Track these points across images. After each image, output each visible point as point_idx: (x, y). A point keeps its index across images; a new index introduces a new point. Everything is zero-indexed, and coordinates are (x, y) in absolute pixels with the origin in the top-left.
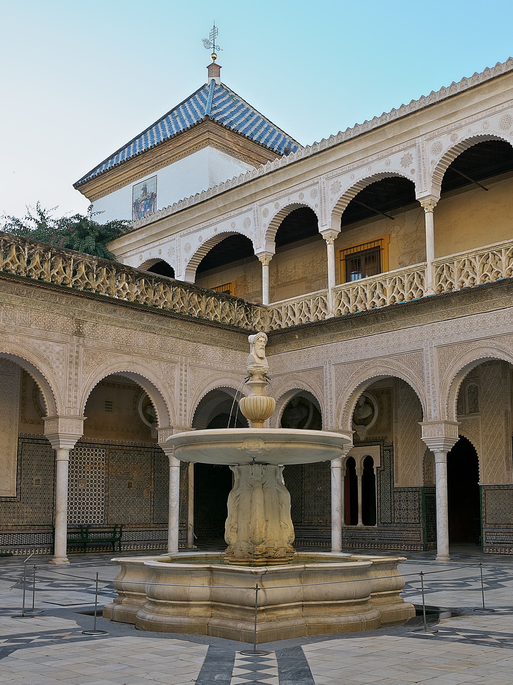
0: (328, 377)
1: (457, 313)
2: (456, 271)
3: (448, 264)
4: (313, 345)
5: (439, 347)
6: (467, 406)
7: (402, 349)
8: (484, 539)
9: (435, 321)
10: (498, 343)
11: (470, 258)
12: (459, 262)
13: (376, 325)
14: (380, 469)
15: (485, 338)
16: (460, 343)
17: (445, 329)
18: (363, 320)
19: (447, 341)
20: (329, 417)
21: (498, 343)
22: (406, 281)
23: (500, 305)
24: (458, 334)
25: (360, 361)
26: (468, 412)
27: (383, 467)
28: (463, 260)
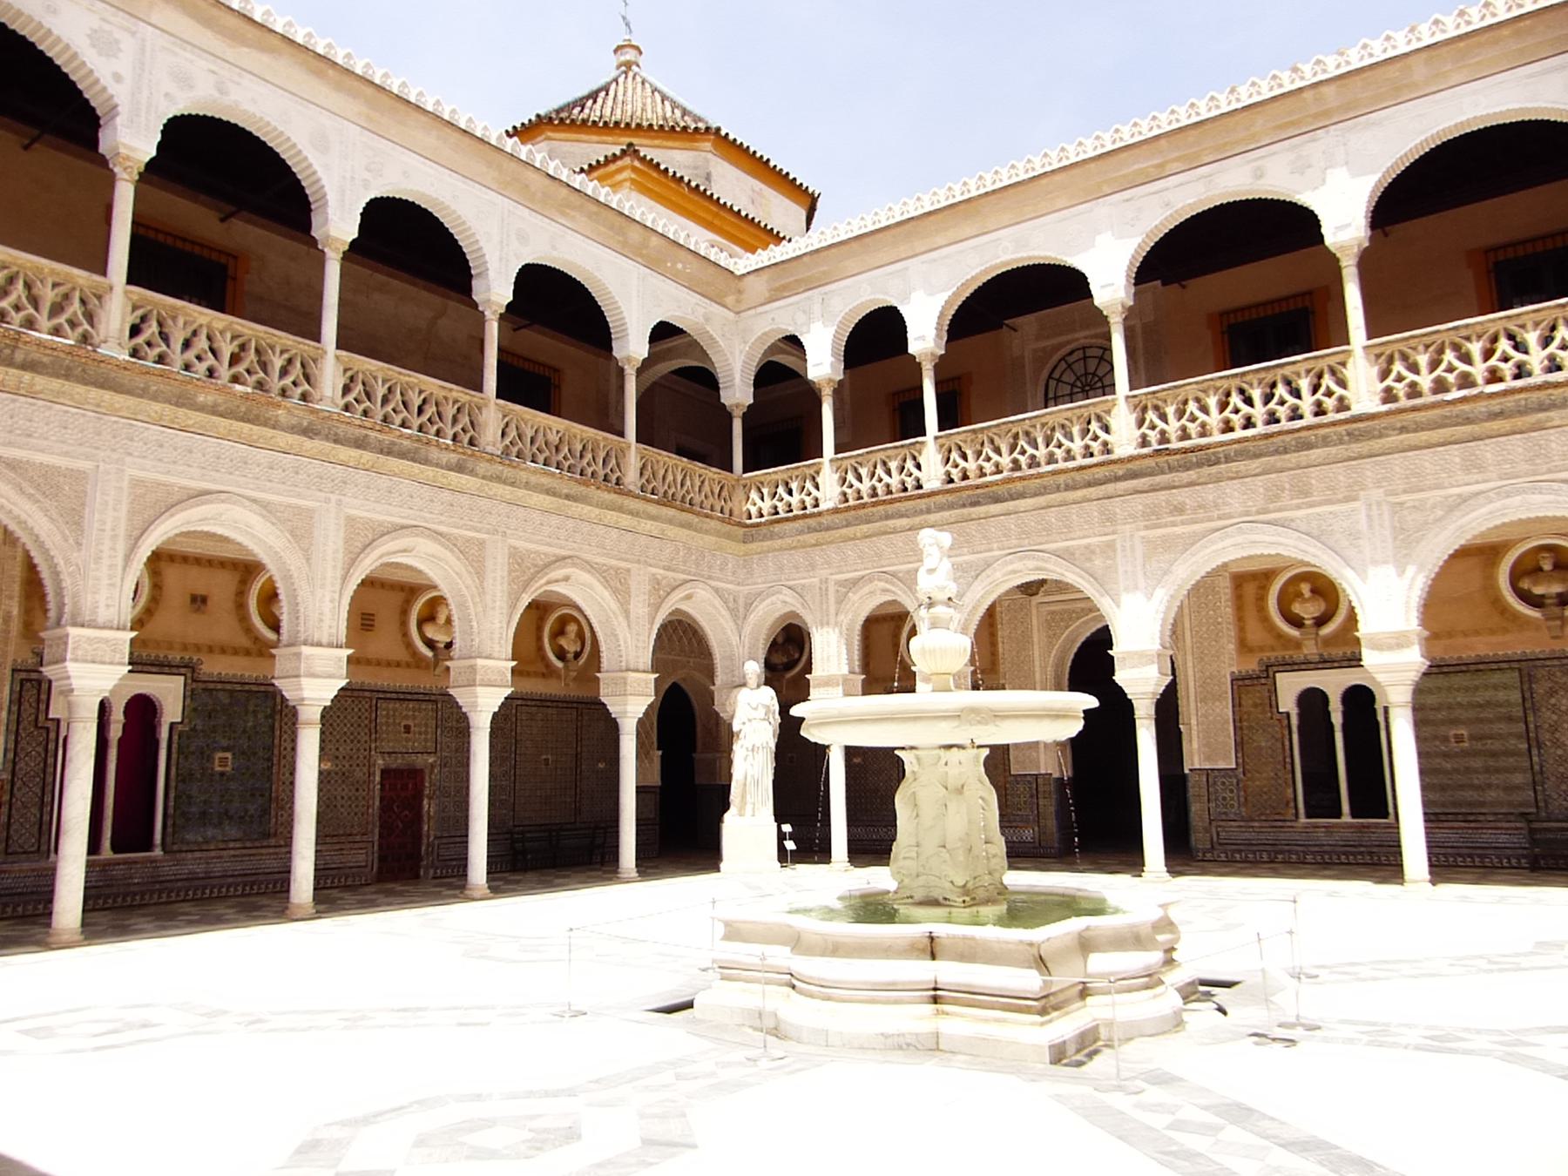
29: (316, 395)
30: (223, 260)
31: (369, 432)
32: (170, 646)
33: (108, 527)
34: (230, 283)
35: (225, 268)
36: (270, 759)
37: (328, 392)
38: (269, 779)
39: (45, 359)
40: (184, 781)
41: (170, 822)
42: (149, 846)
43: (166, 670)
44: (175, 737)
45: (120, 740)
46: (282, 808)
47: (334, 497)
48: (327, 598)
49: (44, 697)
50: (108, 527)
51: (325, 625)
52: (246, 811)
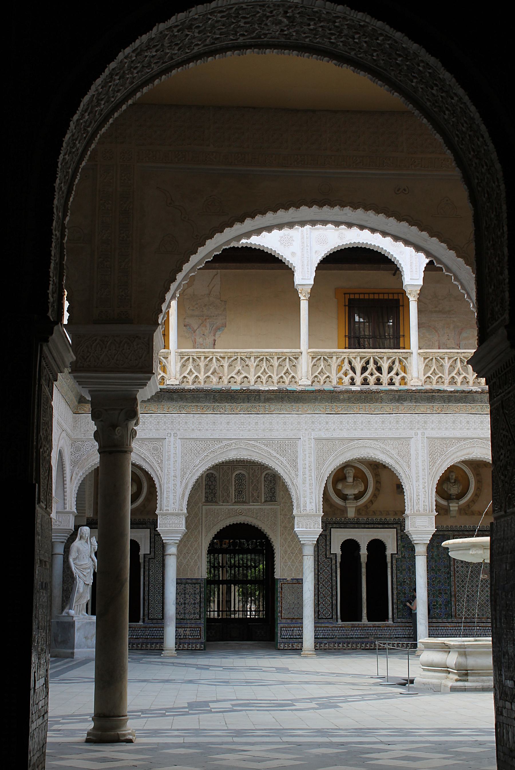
0: (172, 451)
1: (342, 409)
2: (334, 367)
3: (326, 357)
4: (153, 412)
5: (318, 440)
6: (263, 495)
7: (275, 435)
8: (279, 634)
9: (316, 412)
10: (382, 446)
11: (351, 357)
12: (337, 358)
13: (245, 405)
14: (149, 557)
15: (369, 439)
16: (342, 440)
17: (327, 423)
18: (231, 396)
19: (328, 435)
20: (171, 497)
21: (382, 446)
22: (276, 363)
23: (387, 410)
24: (341, 430)
25: (219, 440)
26: (263, 500)
27: (152, 554)
28: (343, 357)
29: (408, 377)
30: (396, 297)
31: (434, 394)
32: (388, 514)
33: (307, 466)
34: (401, 308)
35: (398, 301)
36: (449, 573)
37: (415, 375)
38: (449, 584)
39: (272, 396)
40: (401, 585)
41: (395, 606)
42: (386, 618)
43: (386, 526)
44: (394, 562)
45: (367, 564)
46: (459, 601)
47: (419, 432)
48: (421, 487)
49: (328, 543)
50: (307, 466)
51: (421, 503)
52: (437, 602)
